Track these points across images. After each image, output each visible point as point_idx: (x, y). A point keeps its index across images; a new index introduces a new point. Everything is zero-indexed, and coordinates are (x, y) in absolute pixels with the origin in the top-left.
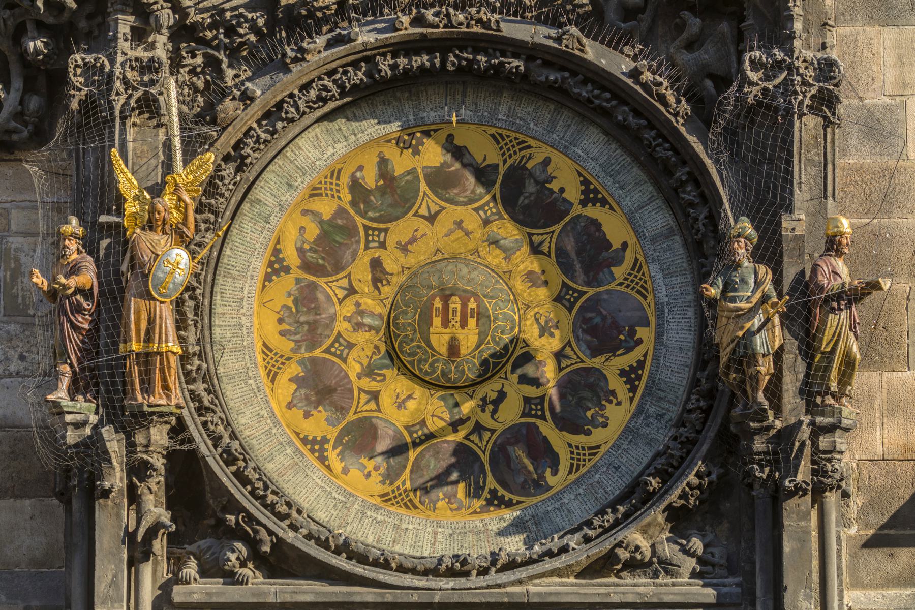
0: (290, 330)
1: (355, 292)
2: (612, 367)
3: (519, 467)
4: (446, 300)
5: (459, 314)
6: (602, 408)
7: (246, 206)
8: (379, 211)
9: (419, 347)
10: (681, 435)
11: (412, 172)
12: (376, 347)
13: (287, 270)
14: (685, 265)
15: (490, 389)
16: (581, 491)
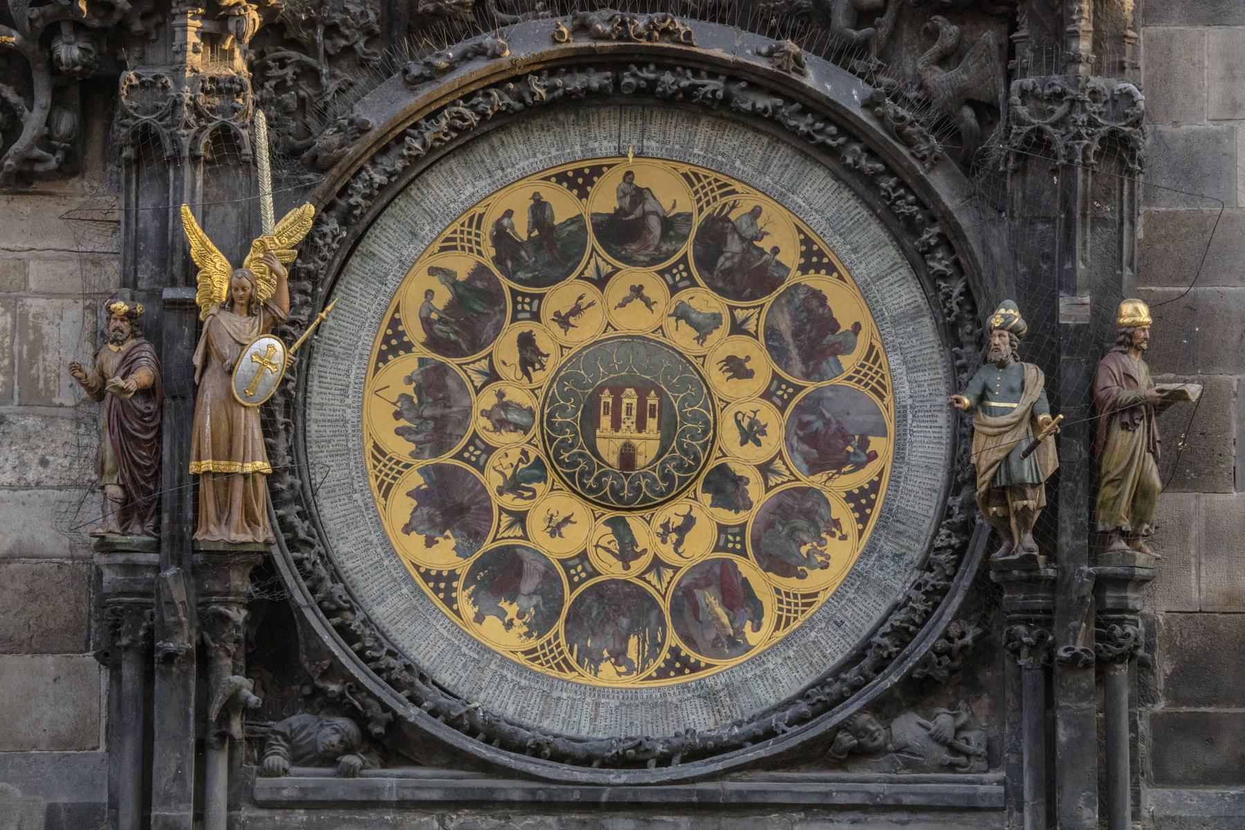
0: (410, 428)
1: (498, 378)
2: (836, 488)
3: (710, 618)
4: (617, 393)
5: (634, 412)
6: (822, 542)
7: (355, 261)
8: (532, 271)
9: (581, 455)
10: (927, 582)
11: (578, 219)
12: (524, 453)
13: (408, 347)
14: (936, 356)
15: (674, 512)
16: (791, 653)
